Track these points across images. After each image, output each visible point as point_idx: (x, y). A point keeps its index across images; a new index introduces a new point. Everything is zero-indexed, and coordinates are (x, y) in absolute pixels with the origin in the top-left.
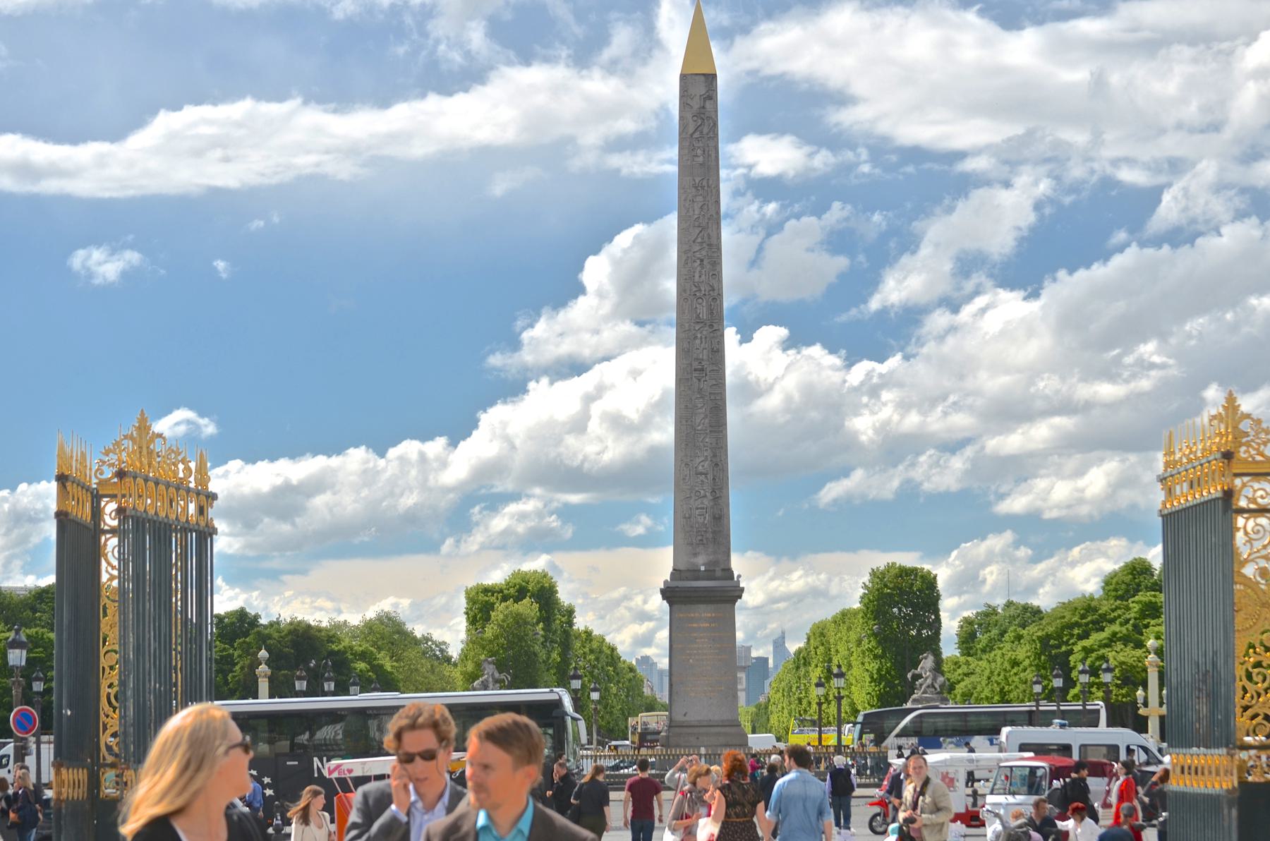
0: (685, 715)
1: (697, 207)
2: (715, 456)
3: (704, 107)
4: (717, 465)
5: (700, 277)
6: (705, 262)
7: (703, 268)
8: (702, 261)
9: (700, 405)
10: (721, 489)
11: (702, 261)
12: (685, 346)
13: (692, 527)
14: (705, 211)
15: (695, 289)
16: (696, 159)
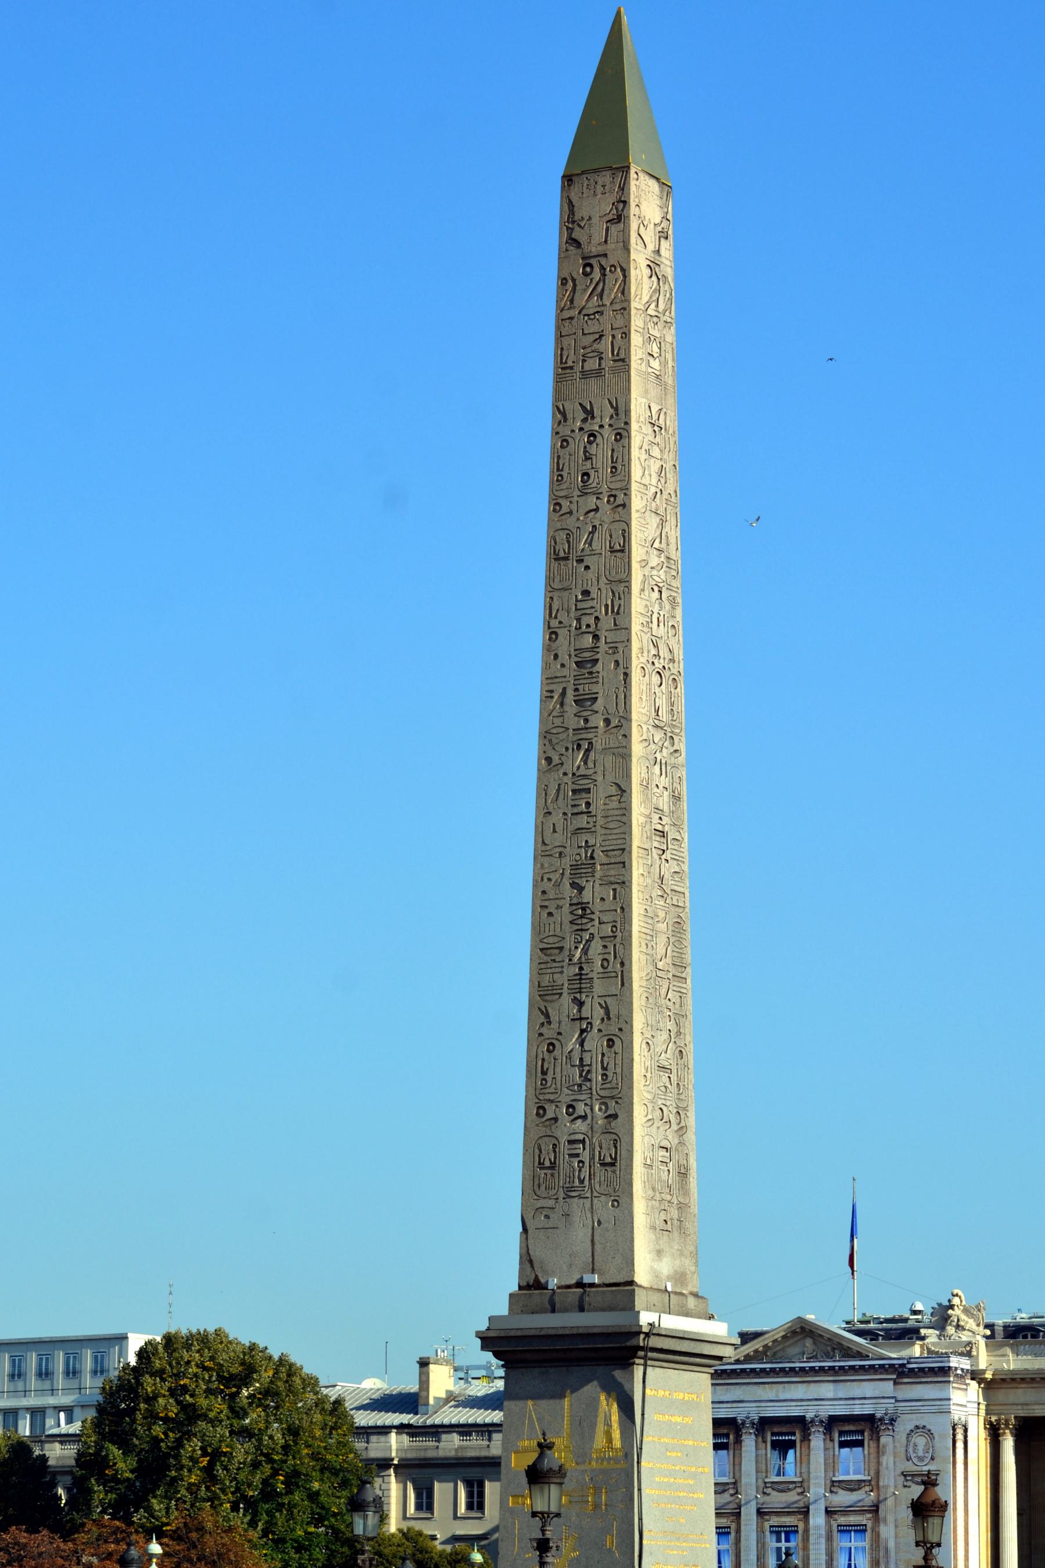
1: (655, 466)
3: (658, 252)
5: (658, 625)
10: (685, 1109)
12: (643, 775)
13: (654, 1189)
14: (663, 481)
15: (653, 652)
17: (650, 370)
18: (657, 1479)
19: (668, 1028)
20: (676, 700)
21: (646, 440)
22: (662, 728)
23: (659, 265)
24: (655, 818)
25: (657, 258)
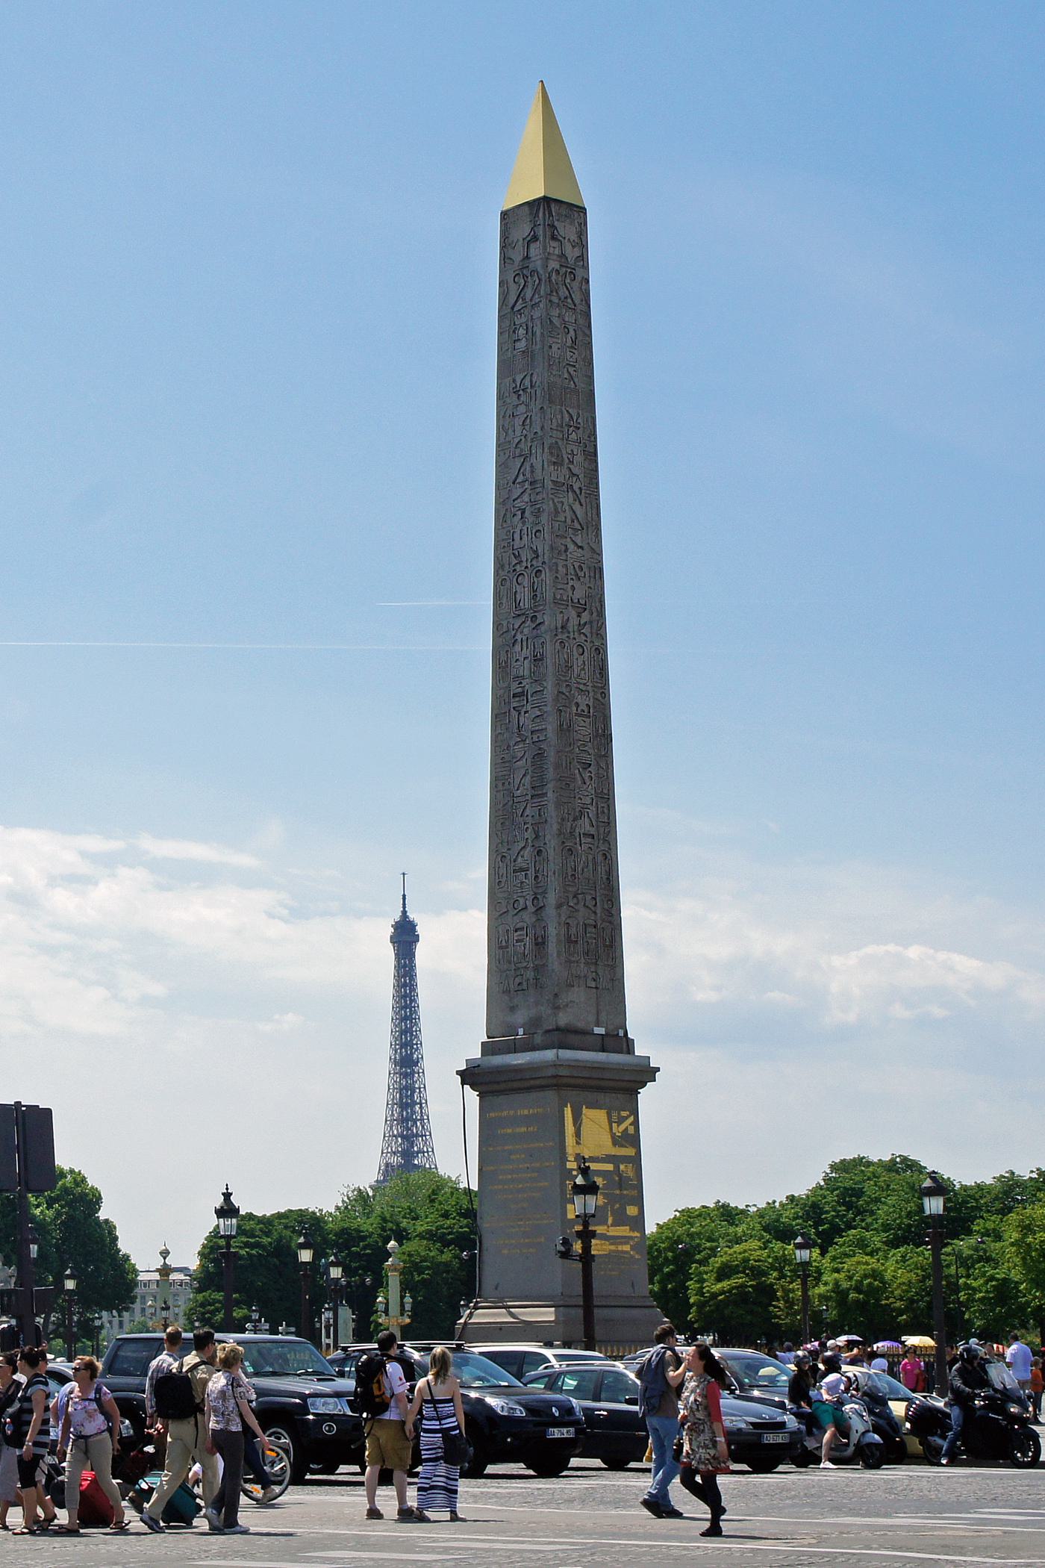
0: (496, 1289)
1: (518, 421)
2: (537, 837)
3: (527, 257)
4: (539, 852)
5: (521, 539)
6: (527, 514)
7: (524, 523)
8: (523, 513)
9: (520, 755)
10: (545, 892)
11: (523, 513)
13: (510, 963)
14: (527, 428)
15: (515, 561)
16: (518, 345)
17: (515, 352)
18: (501, 1177)
19: (526, 837)
20: (540, 584)
21: (511, 407)
22: (523, 614)
23: (528, 267)
24: (514, 686)
25: (526, 261)
